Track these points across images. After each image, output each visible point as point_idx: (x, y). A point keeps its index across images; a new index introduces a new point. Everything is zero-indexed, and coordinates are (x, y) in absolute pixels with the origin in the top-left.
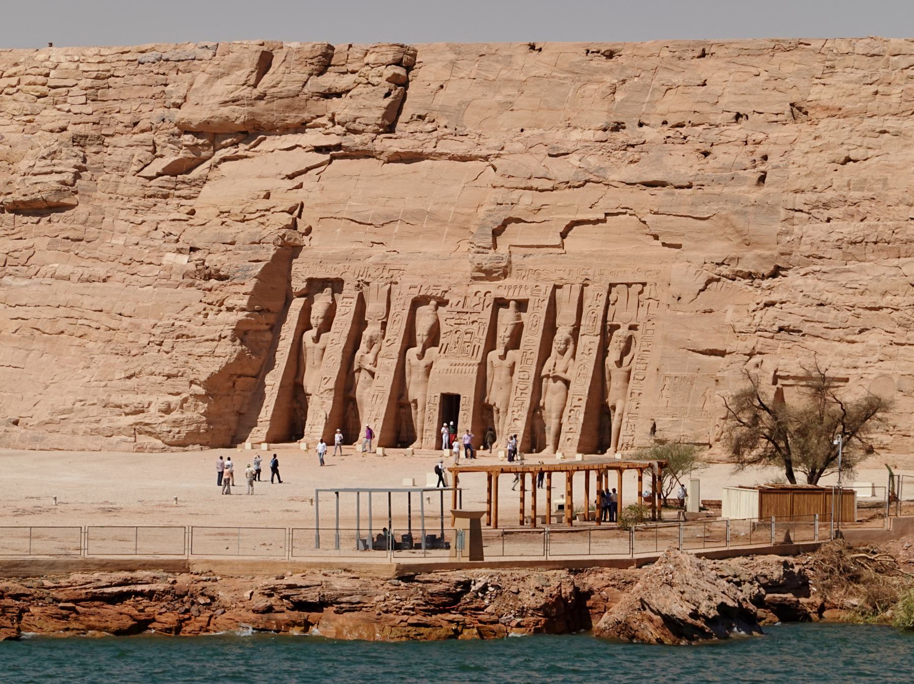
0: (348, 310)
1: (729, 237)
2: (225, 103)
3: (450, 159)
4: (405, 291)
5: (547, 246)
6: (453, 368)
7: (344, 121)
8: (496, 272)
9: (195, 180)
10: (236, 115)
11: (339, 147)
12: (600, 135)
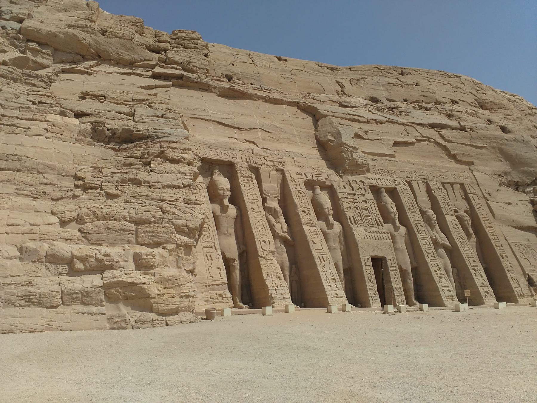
0: (252, 186)
1: (502, 159)
2: (70, 26)
3: (266, 101)
4: (296, 177)
5: (386, 155)
6: (373, 235)
7: (180, 61)
8: (364, 167)
9: (42, 76)
10: (82, 36)
11: (181, 77)
12: (366, 102)
